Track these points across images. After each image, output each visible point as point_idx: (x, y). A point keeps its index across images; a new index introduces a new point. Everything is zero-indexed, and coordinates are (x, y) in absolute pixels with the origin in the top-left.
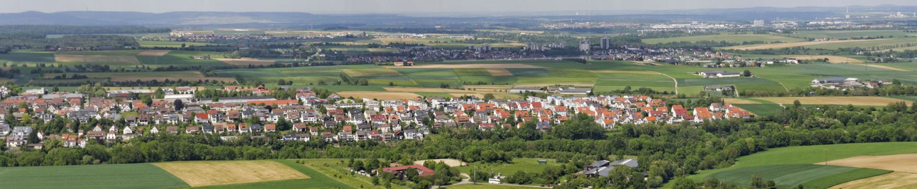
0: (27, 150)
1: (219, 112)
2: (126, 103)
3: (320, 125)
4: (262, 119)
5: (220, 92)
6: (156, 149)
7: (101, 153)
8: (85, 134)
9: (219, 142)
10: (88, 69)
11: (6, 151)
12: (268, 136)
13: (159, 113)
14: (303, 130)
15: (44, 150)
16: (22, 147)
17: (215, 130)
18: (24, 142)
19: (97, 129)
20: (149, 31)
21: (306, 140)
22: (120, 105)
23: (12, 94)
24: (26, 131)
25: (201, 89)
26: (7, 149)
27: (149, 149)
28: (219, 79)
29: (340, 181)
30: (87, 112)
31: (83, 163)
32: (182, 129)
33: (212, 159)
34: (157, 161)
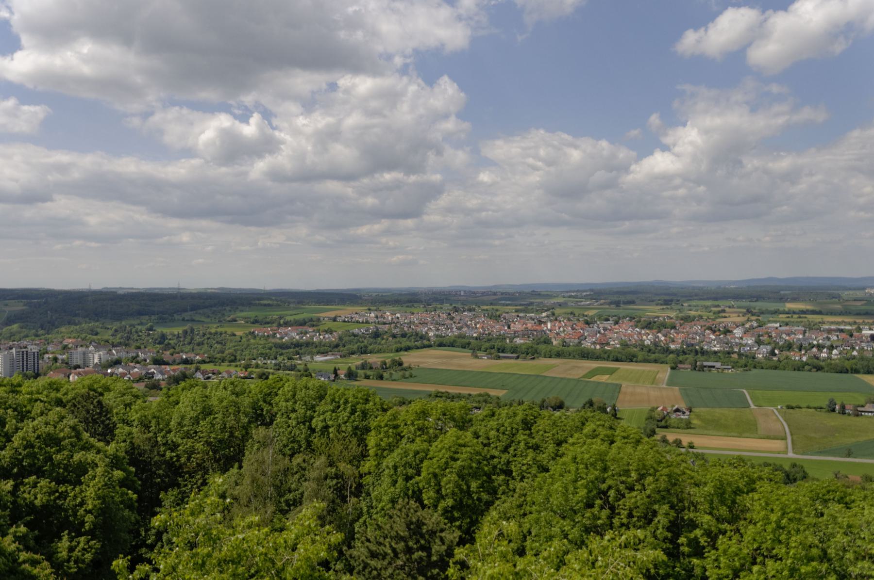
15: (779, 361)
16: (765, 358)
19: (815, 350)
20: (850, 289)
23: (760, 326)
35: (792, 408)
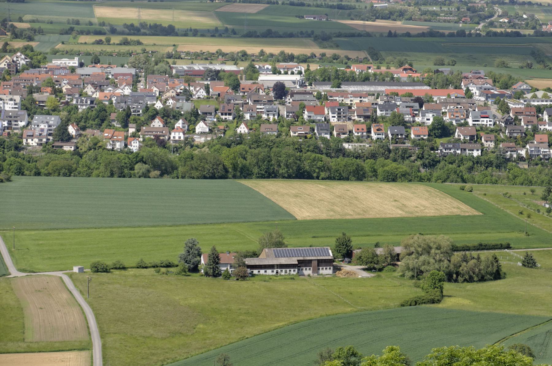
0: (53, 152)
1: (342, 105)
2: (201, 86)
3: (499, 131)
4: (408, 118)
5: (344, 73)
6: (245, 158)
7: (163, 161)
8: (138, 130)
9: (341, 152)
10: (143, 31)
11: (22, 152)
12: (417, 145)
13: (250, 103)
14: (472, 137)
15: (77, 153)
16: (45, 146)
17: (335, 133)
18: (48, 139)
19: (157, 123)
21: (476, 153)
22: (192, 88)
23: (34, 67)
24: (51, 123)
25: (314, 67)
26: (23, 149)
27: (235, 158)
28: (341, 53)
29: (529, 221)
30: (142, 97)
32: (284, 128)
33: (329, 178)
34: (245, 178)
35: (106, 271)
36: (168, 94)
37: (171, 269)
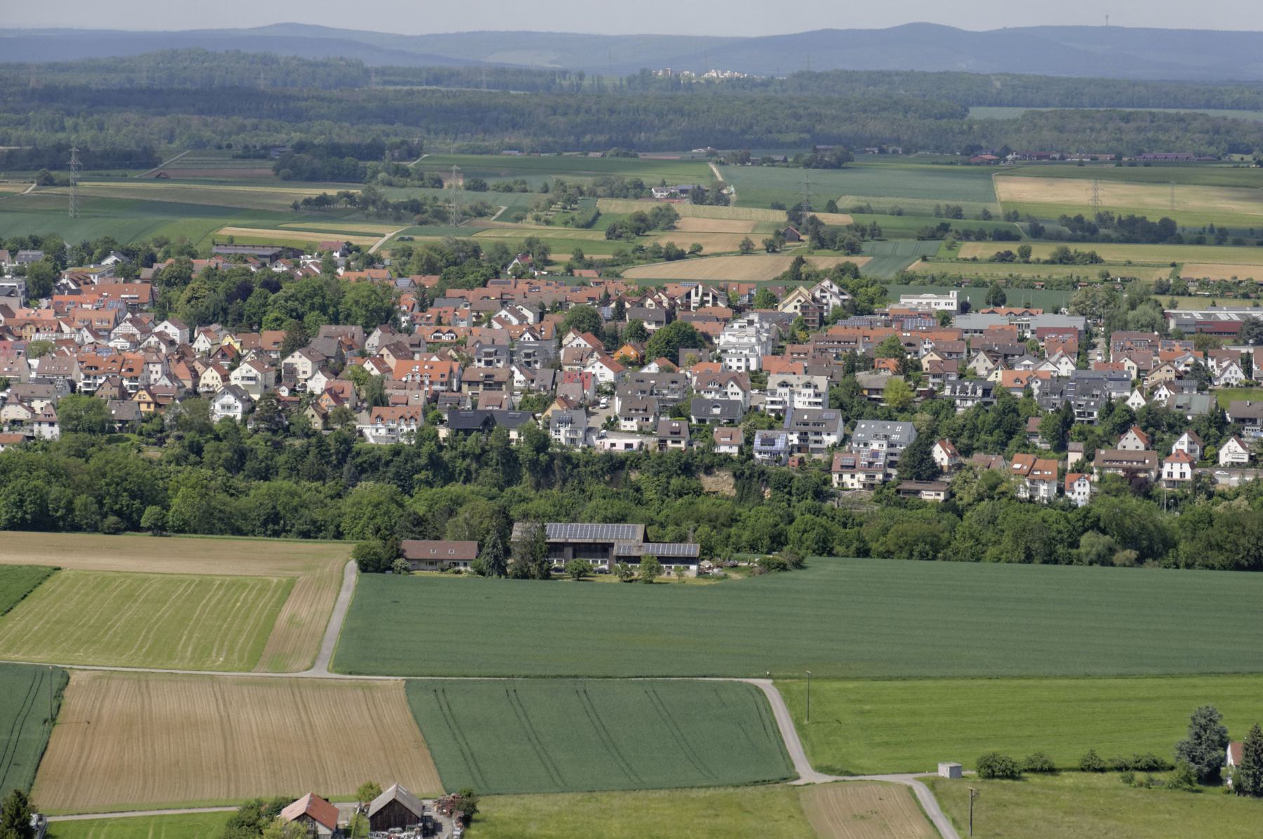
0: (899, 504)
2: (1233, 357)
7: (1143, 528)
8: (1089, 457)
10: (1102, 231)
11: (829, 503)
15: (951, 507)
16: (881, 491)
18: (888, 475)
19: (1132, 441)
22: (1211, 363)
23: (858, 311)
24: (894, 437)
26: (832, 495)
30: (1098, 381)
31: (1080, 560)
35: (1011, 774)
36: (1158, 376)
37: (1157, 776)
